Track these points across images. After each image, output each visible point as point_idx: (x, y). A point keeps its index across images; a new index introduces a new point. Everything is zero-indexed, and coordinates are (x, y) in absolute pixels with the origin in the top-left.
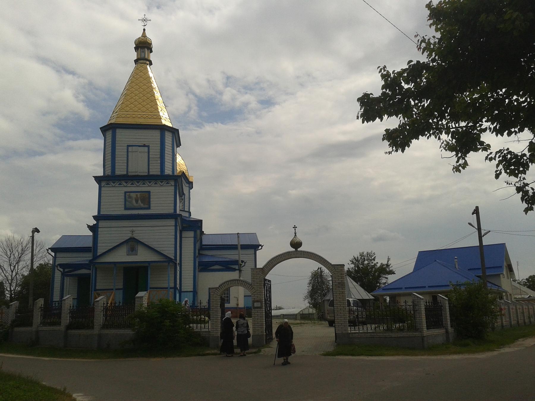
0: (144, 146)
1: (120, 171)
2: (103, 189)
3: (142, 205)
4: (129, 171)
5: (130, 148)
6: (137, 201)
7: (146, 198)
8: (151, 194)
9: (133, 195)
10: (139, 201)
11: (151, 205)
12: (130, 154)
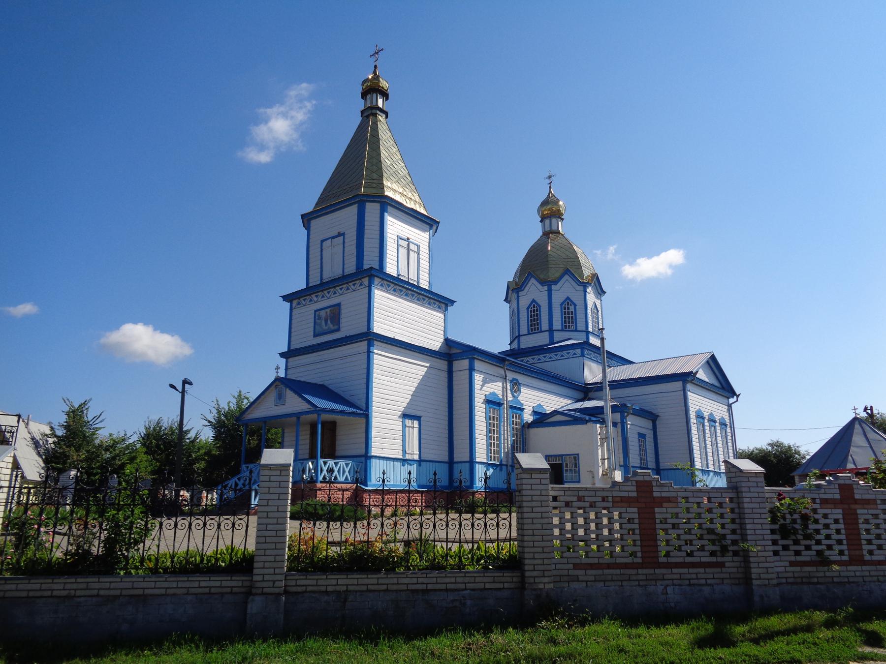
0: (340, 234)
1: (315, 281)
2: (295, 312)
3: (331, 326)
4: (325, 277)
5: (324, 243)
7: (335, 314)
8: (342, 307)
9: (323, 313)
10: (329, 322)
11: (342, 325)
12: (324, 252)
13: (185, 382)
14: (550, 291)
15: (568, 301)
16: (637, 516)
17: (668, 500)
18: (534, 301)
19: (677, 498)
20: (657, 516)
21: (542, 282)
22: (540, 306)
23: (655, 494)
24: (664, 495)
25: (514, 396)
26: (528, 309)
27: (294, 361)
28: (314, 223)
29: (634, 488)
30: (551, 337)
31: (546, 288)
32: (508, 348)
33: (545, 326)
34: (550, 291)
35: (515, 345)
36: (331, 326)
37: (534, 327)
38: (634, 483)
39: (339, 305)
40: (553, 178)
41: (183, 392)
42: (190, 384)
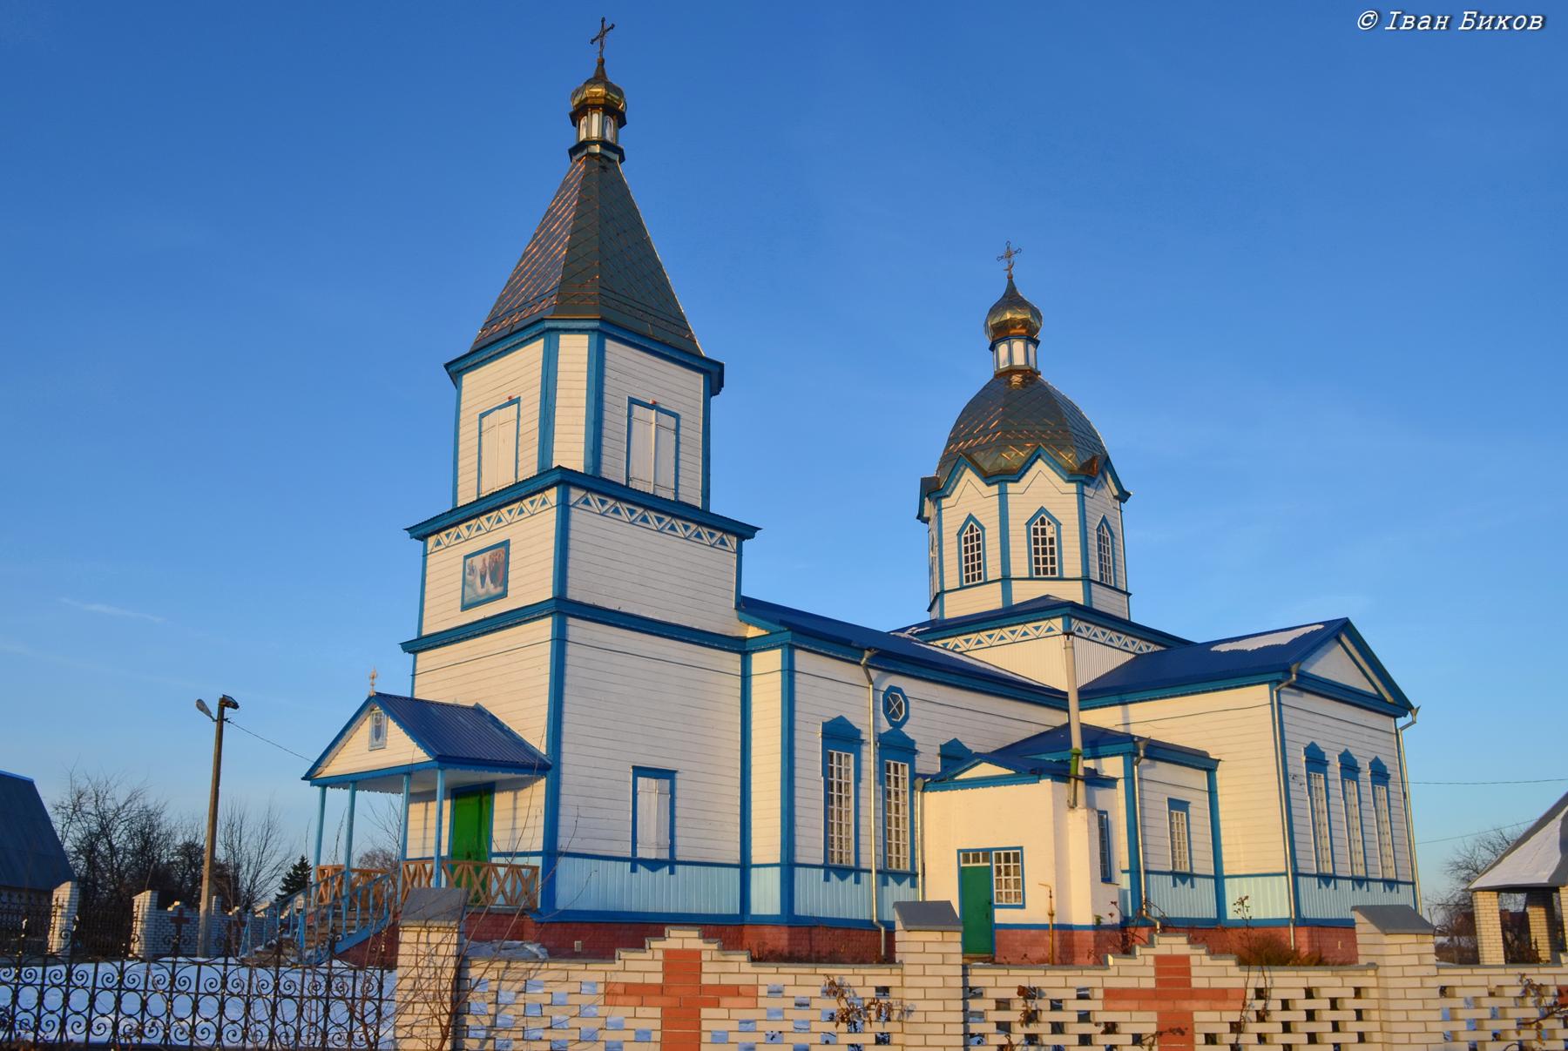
0: (513, 401)
2: (431, 560)
5: (485, 420)
6: (483, 577)
7: (498, 564)
9: (477, 562)
10: (488, 579)
13: (227, 703)
14: (1003, 495)
15: (1042, 517)
16: (657, 1024)
17: (735, 991)
18: (970, 517)
19: (756, 987)
20: (705, 1025)
21: (988, 478)
22: (983, 529)
23: (706, 980)
24: (726, 980)
25: (892, 723)
26: (959, 534)
27: (427, 659)
28: (468, 379)
29: (659, 966)
30: (1007, 593)
31: (995, 489)
32: (926, 617)
33: (993, 570)
34: (1003, 495)
35: (935, 614)
36: (492, 589)
37: (973, 574)
38: (659, 955)
39: (506, 544)
40: (1015, 258)
41: (221, 720)
42: (235, 706)
